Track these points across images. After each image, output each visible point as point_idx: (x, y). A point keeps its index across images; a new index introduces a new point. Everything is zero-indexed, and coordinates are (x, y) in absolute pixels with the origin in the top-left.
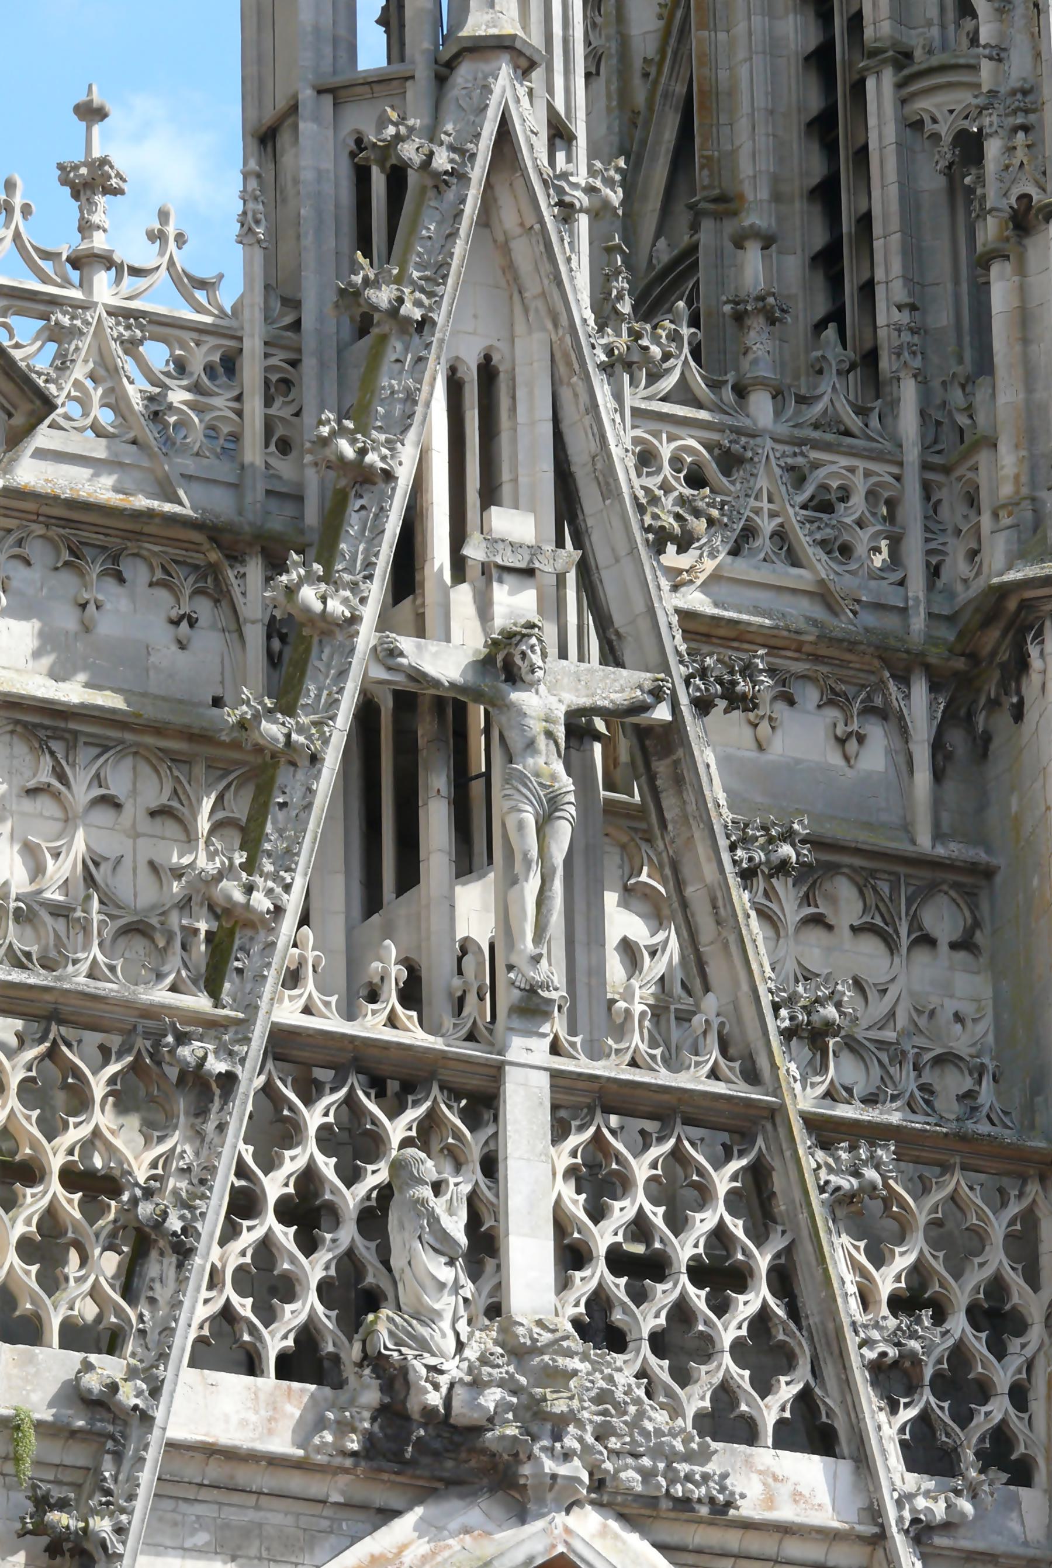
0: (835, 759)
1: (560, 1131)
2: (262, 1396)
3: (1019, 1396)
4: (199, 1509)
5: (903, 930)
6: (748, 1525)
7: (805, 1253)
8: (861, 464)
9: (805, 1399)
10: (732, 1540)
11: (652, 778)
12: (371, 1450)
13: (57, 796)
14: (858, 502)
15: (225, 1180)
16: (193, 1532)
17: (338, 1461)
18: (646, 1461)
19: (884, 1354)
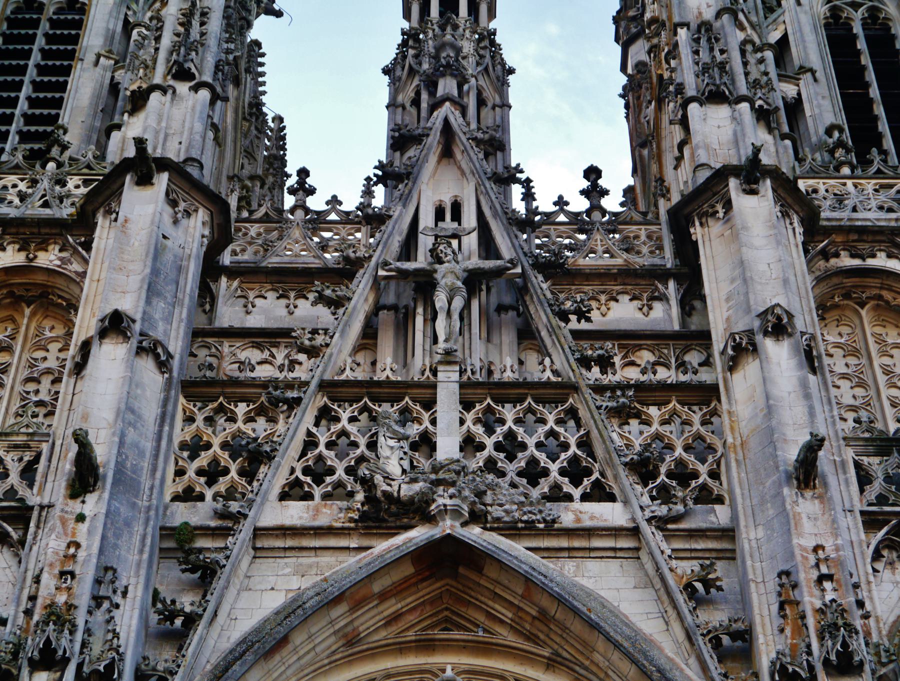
0: (639, 315)
1: (467, 405)
2: (311, 508)
3: (714, 475)
4: (286, 560)
5: (673, 360)
6: (569, 532)
7: (595, 434)
8: (643, 227)
9: (597, 484)
10: (564, 543)
11: (525, 302)
12: (364, 517)
13: (271, 363)
14: (643, 238)
15: (301, 436)
16: (283, 569)
17: (347, 525)
18: (507, 507)
19: (632, 459)
